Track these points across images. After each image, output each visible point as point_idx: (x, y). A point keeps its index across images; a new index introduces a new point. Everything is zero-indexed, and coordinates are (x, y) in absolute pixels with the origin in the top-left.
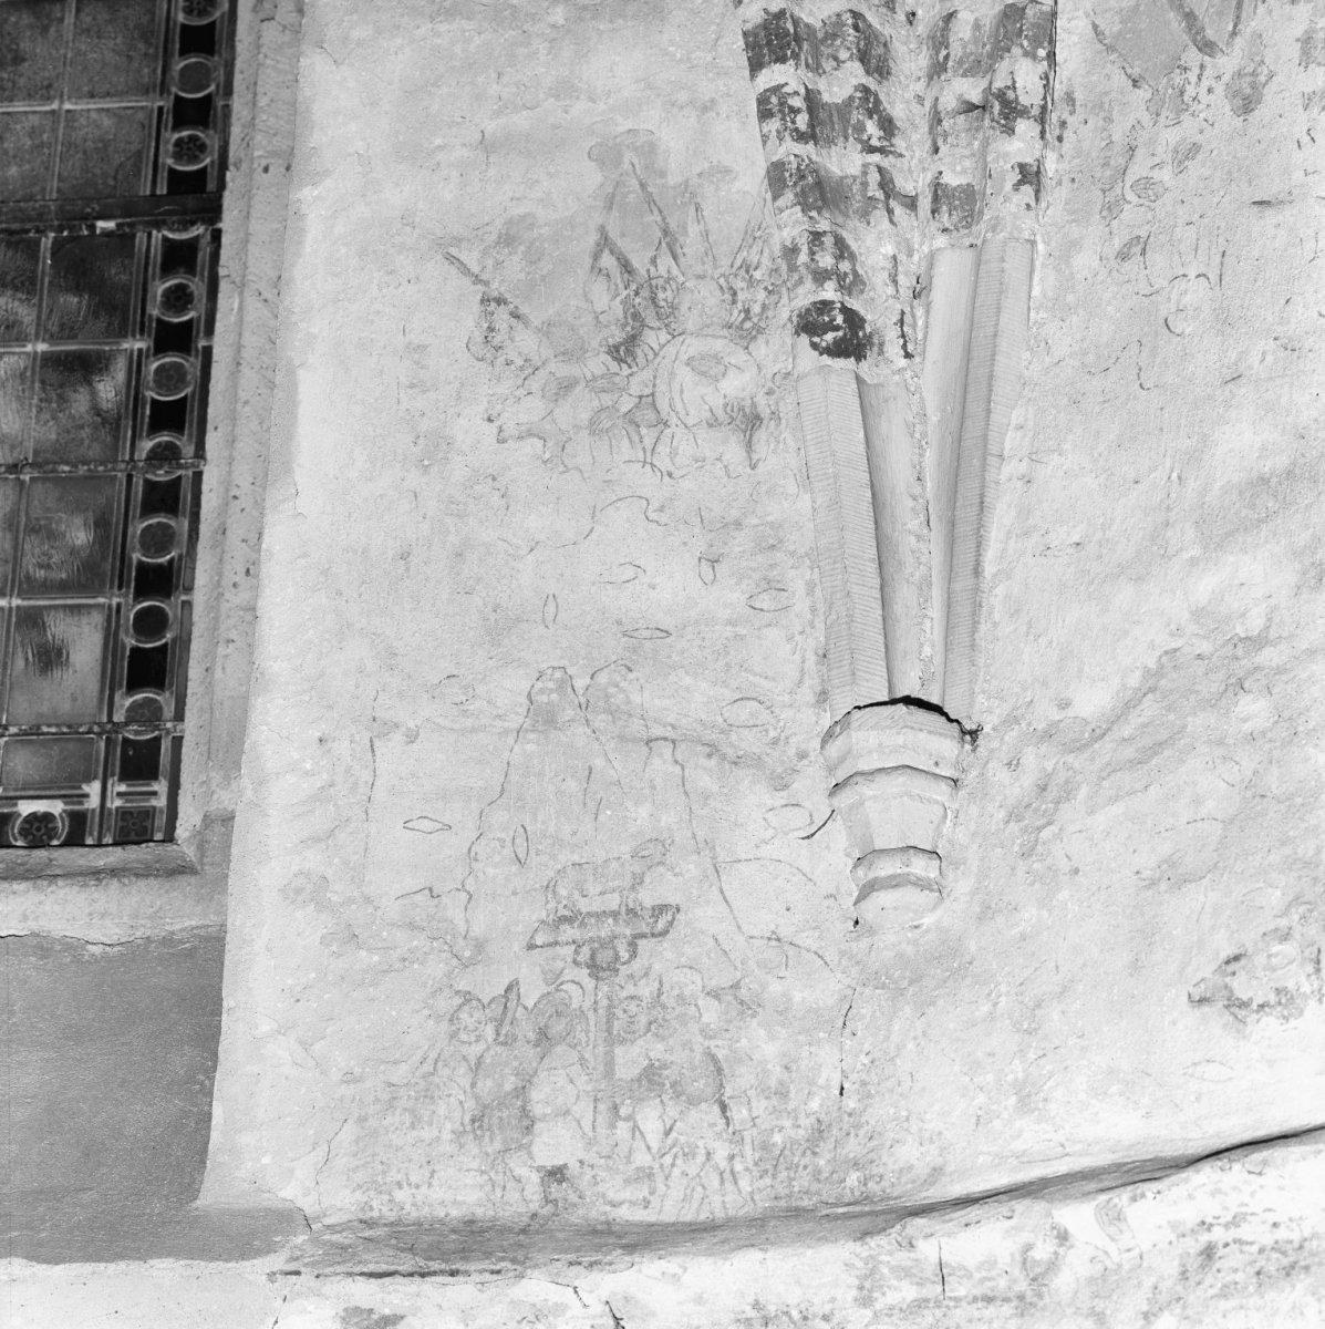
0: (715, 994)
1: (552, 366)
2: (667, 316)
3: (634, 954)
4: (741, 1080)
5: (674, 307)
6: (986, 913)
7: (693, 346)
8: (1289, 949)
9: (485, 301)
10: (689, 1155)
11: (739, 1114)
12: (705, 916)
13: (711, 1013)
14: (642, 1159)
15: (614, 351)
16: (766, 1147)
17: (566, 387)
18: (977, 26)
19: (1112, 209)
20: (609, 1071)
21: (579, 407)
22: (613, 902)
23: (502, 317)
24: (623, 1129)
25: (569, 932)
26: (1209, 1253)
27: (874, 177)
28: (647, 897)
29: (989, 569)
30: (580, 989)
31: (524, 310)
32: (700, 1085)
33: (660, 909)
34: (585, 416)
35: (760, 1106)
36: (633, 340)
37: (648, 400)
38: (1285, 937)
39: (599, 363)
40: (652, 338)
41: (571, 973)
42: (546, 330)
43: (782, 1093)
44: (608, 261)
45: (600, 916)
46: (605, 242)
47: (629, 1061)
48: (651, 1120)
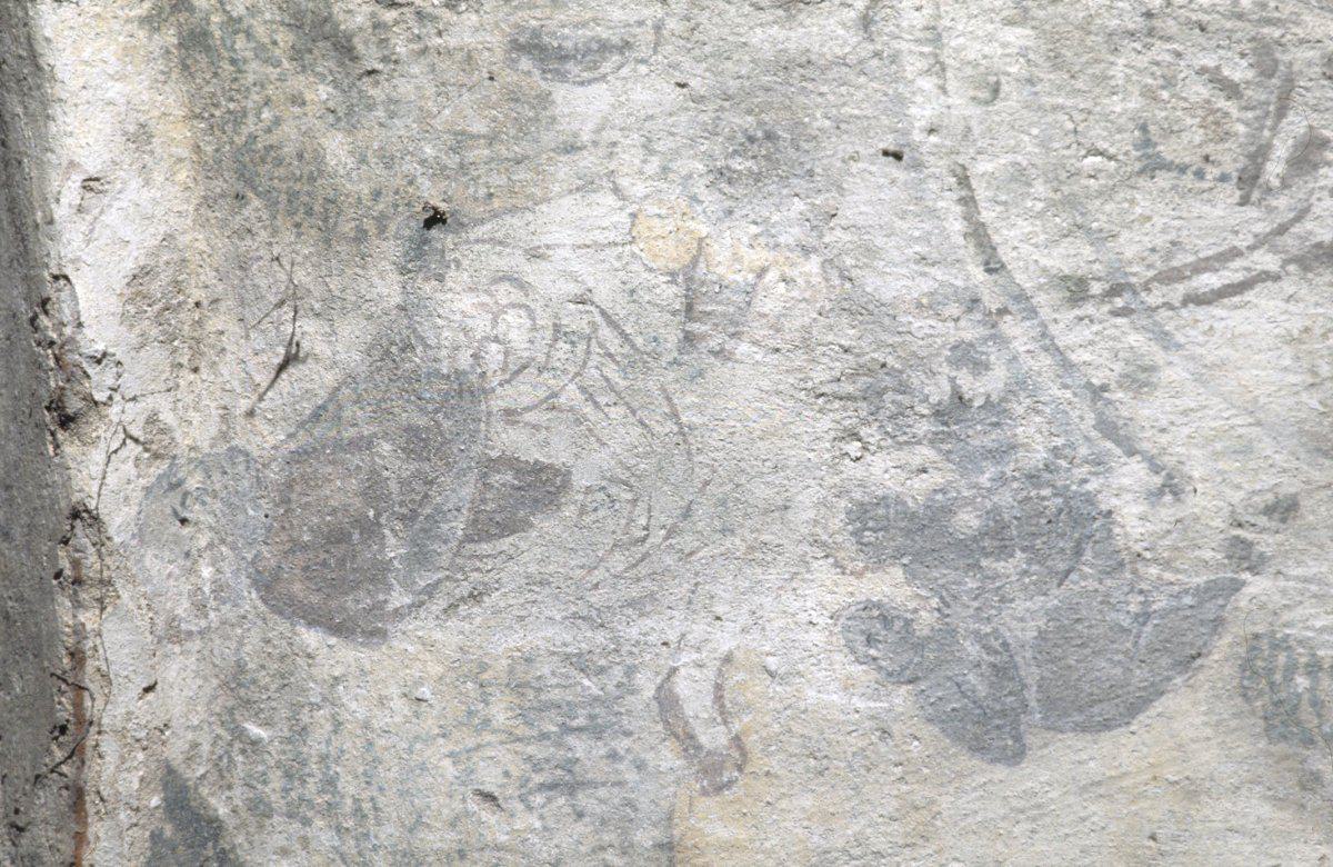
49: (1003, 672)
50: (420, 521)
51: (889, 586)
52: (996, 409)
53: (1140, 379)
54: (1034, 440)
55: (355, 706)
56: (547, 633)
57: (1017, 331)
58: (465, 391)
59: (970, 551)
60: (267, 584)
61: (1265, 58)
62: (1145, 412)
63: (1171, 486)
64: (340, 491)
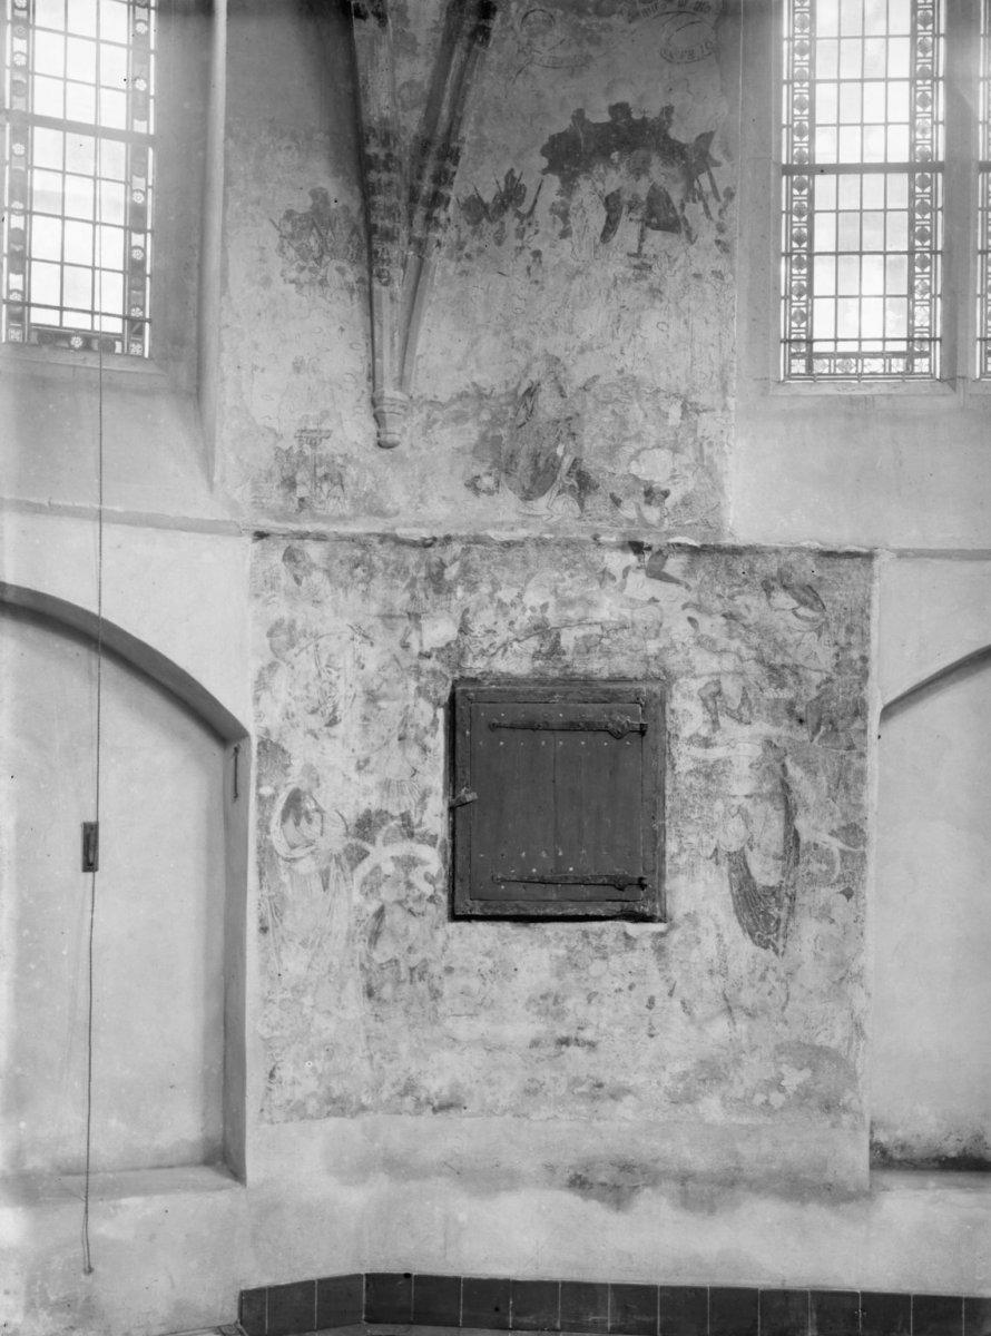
4: (347, 480)
9: (281, 236)
12: (338, 434)
15: (315, 259)
16: (353, 498)
17: (303, 269)
19: (459, 260)
22: (316, 427)
24: (318, 490)
25: (304, 435)
28: (324, 427)
30: (308, 451)
32: (336, 480)
33: (328, 431)
35: (352, 488)
41: (305, 445)
43: (357, 484)
45: (312, 431)
47: (320, 472)
48: (326, 487)
51: (286, 623)
55: (276, 557)
58: (310, 574)
59: (290, 632)
62: (304, 654)
63: (296, 656)
64: (299, 558)
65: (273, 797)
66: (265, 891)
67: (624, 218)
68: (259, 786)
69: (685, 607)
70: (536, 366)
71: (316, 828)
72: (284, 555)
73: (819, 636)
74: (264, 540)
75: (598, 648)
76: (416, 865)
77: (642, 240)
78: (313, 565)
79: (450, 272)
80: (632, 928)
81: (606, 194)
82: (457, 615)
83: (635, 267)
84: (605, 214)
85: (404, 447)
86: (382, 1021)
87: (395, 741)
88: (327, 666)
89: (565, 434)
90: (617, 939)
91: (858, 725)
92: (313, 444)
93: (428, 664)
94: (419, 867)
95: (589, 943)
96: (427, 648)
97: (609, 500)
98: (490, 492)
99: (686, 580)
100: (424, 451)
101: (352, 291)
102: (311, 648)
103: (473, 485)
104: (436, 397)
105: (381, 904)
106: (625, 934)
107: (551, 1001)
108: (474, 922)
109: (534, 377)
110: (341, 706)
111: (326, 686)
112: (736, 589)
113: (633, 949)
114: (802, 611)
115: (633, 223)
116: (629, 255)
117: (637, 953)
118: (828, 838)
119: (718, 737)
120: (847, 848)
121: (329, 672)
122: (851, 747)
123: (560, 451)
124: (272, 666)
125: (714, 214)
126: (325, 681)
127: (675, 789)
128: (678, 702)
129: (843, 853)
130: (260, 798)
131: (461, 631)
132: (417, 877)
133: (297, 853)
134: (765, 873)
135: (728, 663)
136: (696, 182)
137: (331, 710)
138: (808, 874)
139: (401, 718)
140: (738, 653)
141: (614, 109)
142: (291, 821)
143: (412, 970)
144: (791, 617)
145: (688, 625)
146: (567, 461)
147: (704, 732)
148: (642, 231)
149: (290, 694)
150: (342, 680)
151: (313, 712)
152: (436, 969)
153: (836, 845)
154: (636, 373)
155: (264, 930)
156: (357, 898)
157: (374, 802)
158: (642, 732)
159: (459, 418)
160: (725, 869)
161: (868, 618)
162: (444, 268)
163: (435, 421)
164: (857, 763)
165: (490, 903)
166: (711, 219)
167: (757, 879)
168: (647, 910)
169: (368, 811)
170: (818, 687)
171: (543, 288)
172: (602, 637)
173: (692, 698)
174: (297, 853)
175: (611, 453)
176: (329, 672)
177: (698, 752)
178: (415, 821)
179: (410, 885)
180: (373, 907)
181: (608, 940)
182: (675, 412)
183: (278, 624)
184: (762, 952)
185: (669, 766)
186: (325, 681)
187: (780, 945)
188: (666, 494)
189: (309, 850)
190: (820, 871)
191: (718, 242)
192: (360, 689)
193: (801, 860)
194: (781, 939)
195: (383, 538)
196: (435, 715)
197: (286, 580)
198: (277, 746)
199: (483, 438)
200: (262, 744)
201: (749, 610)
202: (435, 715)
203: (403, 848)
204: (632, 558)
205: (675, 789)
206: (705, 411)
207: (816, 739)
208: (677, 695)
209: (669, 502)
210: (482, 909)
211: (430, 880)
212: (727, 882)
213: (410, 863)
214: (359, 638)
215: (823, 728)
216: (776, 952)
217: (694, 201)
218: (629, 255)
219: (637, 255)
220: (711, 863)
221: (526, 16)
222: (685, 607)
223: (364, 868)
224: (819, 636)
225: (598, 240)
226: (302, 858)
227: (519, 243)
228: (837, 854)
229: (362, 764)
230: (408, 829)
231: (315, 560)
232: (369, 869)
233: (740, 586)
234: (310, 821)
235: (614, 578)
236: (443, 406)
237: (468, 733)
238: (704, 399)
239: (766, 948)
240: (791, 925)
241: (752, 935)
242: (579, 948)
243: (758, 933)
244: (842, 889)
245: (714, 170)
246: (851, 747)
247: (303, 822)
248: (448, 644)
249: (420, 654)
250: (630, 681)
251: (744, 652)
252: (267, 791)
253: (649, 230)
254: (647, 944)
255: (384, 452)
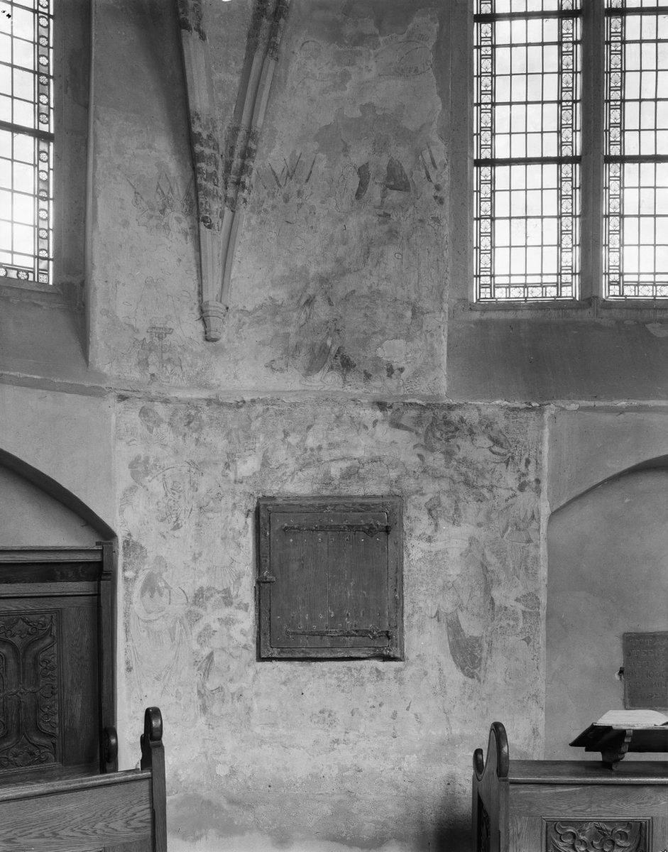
0: (180, 346)
1: (149, 211)
2: (171, 206)
3: (166, 336)
5: (172, 204)
6: (229, 341)
7: (176, 215)
8: (283, 361)
10: (175, 375)
11: (184, 369)
12: (178, 331)
13: (179, 350)
14: (168, 374)
17: (151, 217)
18: (237, 165)
19: (259, 213)
20: (162, 358)
21: (153, 222)
22: (162, 326)
23: (139, 198)
25: (154, 330)
26: (268, 409)
27: (215, 191)
29: (232, 277)
30: (156, 341)
31: (143, 197)
33: (170, 329)
34: (155, 225)
35: (188, 368)
36: (164, 210)
37: (167, 224)
38: (282, 359)
39: (158, 213)
40: (168, 210)
42: (147, 203)
44: (159, 190)
46: (158, 186)
47: (166, 356)
49: (136, 467)
50: (149, 421)
51: (142, 459)
52: (156, 469)
53: (158, 480)
54: (154, 471)
56: (140, 431)
57: (161, 471)
58: (159, 426)
60: (143, 407)
61: (181, 491)
62: (155, 480)
63: (150, 481)
64: (151, 414)
65: (135, 578)
66: (130, 643)
67: (371, 183)
68: (124, 570)
69: (415, 446)
70: (312, 284)
71: (165, 599)
72: (140, 412)
73: (507, 466)
74: (126, 401)
75: (357, 475)
76: (234, 624)
77: (383, 197)
78: (161, 420)
79: (253, 222)
80: (381, 665)
81: (359, 165)
82: (260, 454)
83: (380, 215)
84: (359, 179)
85: (223, 340)
86: (213, 728)
87: (219, 541)
88: (172, 489)
89: (333, 331)
90: (371, 673)
91: (534, 525)
92: (160, 338)
93: (240, 488)
94: (237, 624)
95: (352, 675)
96: (239, 476)
97: (363, 375)
98: (281, 370)
99: (416, 428)
100: (237, 344)
101: (186, 234)
102: (160, 477)
103: (271, 366)
104: (244, 307)
105: (211, 650)
106: (377, 670)
107: (326, 715)
108: (274, 661)
109: (310, 292)
110: (182, 516)
111: (171, 503)
112: (450, 434)
113: (382, 679)
114: (496, 449)
115: (377, 186)
116: (375, 207)
117: (385, 682)
118: (514, 603)
119: (438, 535)
120: (527, 610)
121: (174, 494)
122: (529, 541)
123: (329, 343)
124: (132, 489)
125: (433, 178)
126: (170, 500)
127: (409, 571)
128: (411, 511)
129: (524, 612)
130: (126, 579)
131: (263, 465)
132: (235, 631)
133: (152, 617)
134: (471, 628)
135: (445, 485)
136: (420, 157)
137: (175, 519)
138: (501, 627)
139: (223, 524)
140: (451, 478)
141: (363, 108)
142: (148, 594)
143: (233, 694)
144: (489, 453)
145: (418, 459)
146: (334, 349)
147: (429, 532)
148: (384, 190)
149: (145, 508)
150: (182, 499)
151: (162, 521)
152: (247, 694)
153: (520, 607)
154: (381, 288)
155: (129, 669)
156: (196, 647)
157: (204, 582)
158: (387, 530)
159: (259, 321)
160: (444, 626)
161: (541, 453)
162: (249, 220)
163: (244, 323)
164: (533, 553)
165: (284, 650)
166: (431, 181)
167: (466, 631)
168: (392, 653)
169: (202, 588)
170: (506, 500)
171: (316, 232)
172: (359, 468)
173: (420, 509)
174: (152, 617)
175: (364, 343)
176: (174, 494)
177: (424, 545)
178: (234, 593)
179: (230, 637)
180: (206, 652)
181: (365, 674)
182: (409, 314)
183: (137, 459)
184: (470, 681)
185: (405, 555)
186: (170, 500)
187: (481, 675)
188: (401, 370)
189: (160, 615)
190: (509, 625)
191: (436, 197)
192: (195, 505)
193: (496, 618)
194: (483, 671)
195: (209, 401)
196: (246, 522)
197: (141, 429)
198: (135, 545)
199: (276, 335)
200: (127, 542)
201: (459, 449)
202: (246, 522)
203: (225, 612)
204: (379, 414)
205: (409, 571)
206: (428, 313)
207: (506, 535)
208: (410, 507)
209: (404, 375)
210: (279, 653)
211: (243, 633)
212: (446, 634)
213: (228, 622)
214: (194, 470)
215: (510, 528)
216: (479, 681)
217: (419, 170)
218: (375, 207)
219: (379, 208)
220: (435, 621)
221: (303, 45)
222: (415, 446)
223: (198, 628)
224: (507, 466)
225: (354, 198)
226: (156, 620)
227: (298, 201)
228: (520, 613)
229: (197, 556)
230: (227, 600)
231: (163, 417)
232: (202, 627)
233: (453, 432)
234: (161, 594)
235: (366, 427)
236: (249, 313)
237: (268, 534)
238: (427, 304)
239: (473, 677)
240: (489, 662)
241: (462, 669)
242: (346, 678)
243: (467, 668)
244: (524, 637)
245: (431, 147)
246: (529, 541)
247: (156, 594)
248: (254, 474)
249: (235, 481)
250: (378, 497)
251: (456, 477)
252: (129, 574)
253: (388, 190)
254: (391, 676)
255: (211, 344)
